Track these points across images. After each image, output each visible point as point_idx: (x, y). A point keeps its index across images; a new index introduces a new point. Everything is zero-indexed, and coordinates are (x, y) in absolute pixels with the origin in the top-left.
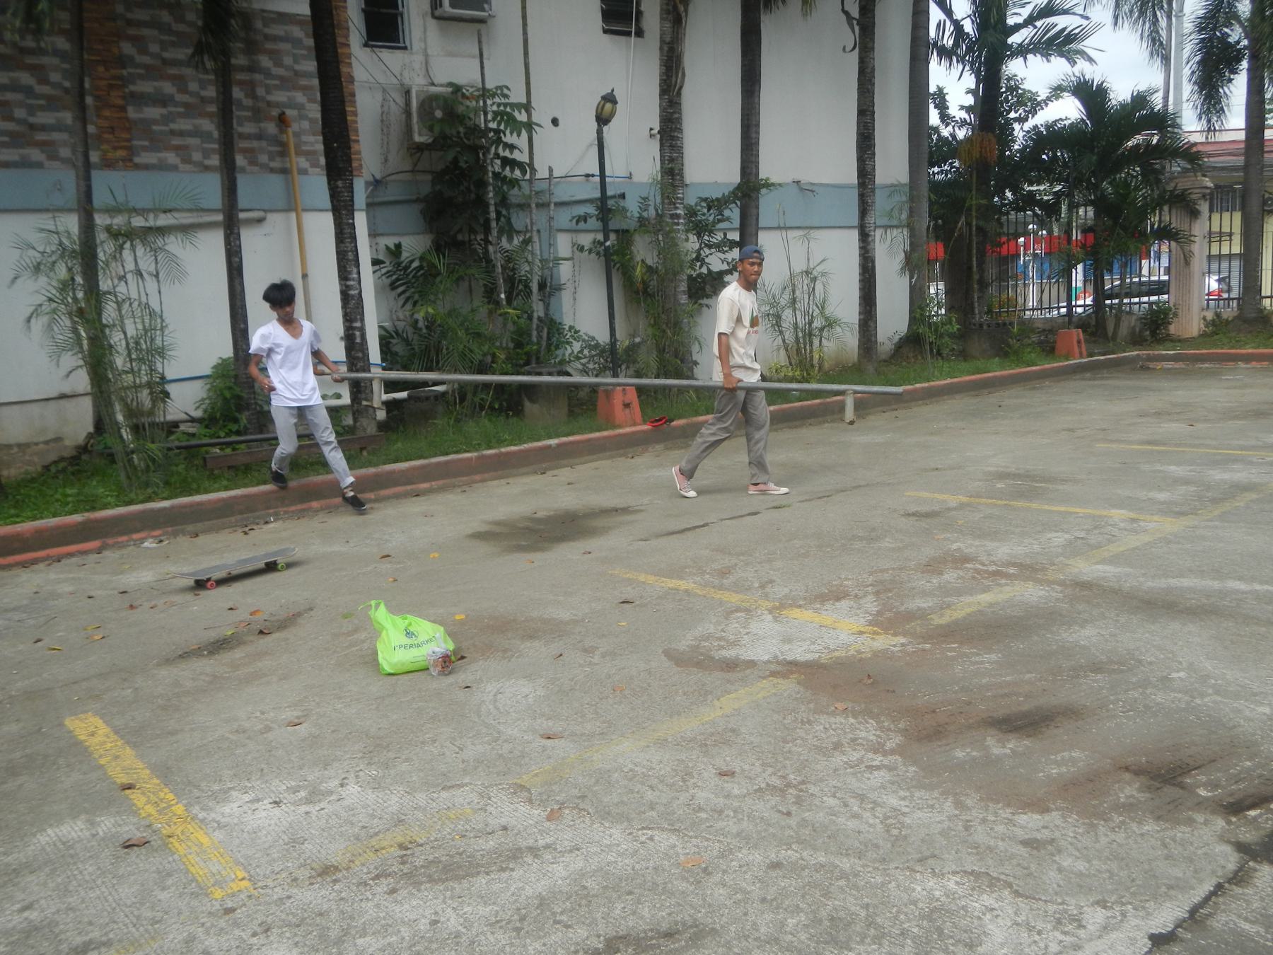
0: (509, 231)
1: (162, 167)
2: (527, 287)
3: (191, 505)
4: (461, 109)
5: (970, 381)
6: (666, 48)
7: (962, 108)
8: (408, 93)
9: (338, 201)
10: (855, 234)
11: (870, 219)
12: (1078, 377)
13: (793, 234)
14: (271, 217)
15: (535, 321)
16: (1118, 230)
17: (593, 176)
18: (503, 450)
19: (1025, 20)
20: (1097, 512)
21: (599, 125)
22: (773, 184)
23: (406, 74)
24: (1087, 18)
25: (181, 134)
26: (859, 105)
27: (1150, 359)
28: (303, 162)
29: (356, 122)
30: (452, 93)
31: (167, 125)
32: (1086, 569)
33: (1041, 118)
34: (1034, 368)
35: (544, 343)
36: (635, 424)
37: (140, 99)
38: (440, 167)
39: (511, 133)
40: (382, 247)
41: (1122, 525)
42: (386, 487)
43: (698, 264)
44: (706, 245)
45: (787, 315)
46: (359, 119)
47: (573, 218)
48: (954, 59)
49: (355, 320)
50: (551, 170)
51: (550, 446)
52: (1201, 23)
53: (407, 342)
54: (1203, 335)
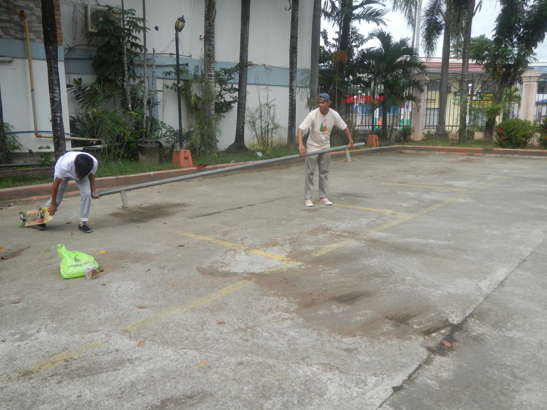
0: (134, 77)
2: (142, 102)
7: (334, 39)
8: (86, 8)
9: (50, 56)
10: (288, 89)
11: (294, 84)
12: (375, 154)
15: (145, 118)
16: (393, 95)
17: (174, 54)
18: (128, 176)
19: (360, 4)
20: (380, 211)
21: (176, 31)
22: (253, 65)
24: (384, 6)
27: (403, 148)
28: (32, 36)
29: (60, 19)
30: (108, 10)
32: (375, 234)
33: (365, 46)
34: (358, 150)
35: (149, 129)
36: (189, 167)
38: (101, 44)
40: (72, 79)
41: (389, 216)
43: (220, 97)
44: (224, 89)
45: (258, 122)
46: (61, 18)
47: (164, 73)
49: (58, 113)
50: (154, 50)
51: (150, 175)
52: (427, 13)
53: (83, 124)
54: (423, 140)
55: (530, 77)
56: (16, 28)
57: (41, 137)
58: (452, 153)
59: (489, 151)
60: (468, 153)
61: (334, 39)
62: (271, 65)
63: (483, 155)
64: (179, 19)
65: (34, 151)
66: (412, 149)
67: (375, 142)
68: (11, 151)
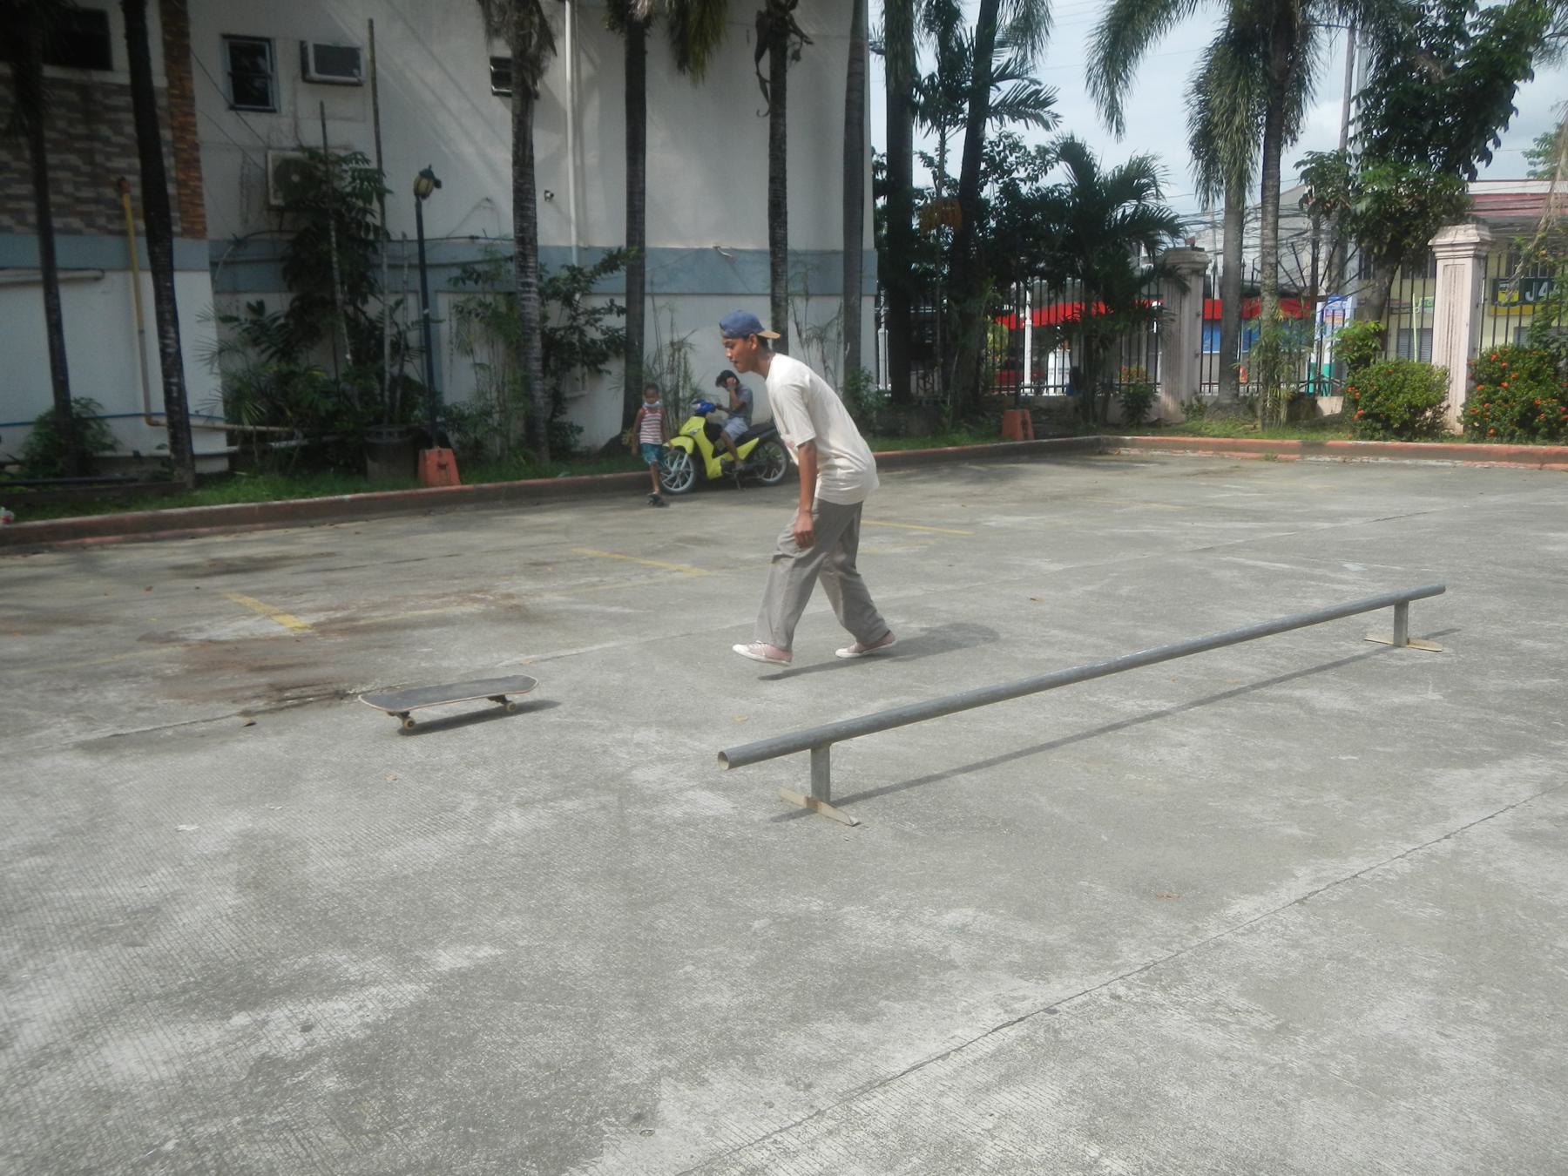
14: (108, 275)
18: (292, 501)
21: (418, 199)
25: (18, 198)
26: (771, 172)
27: (1109, 444)
36: (450, 484)
51: (342, 501)
55: (1452, 245)
56: (110, 212)
58: (1226, 454)
59: (1318, 448)
60: (1263, 455)
62: (735, 247)
63: (1302, 458)
65: (144, 453)
66: (1133, 444)
67: (1019, 427)
68: (95, 454)
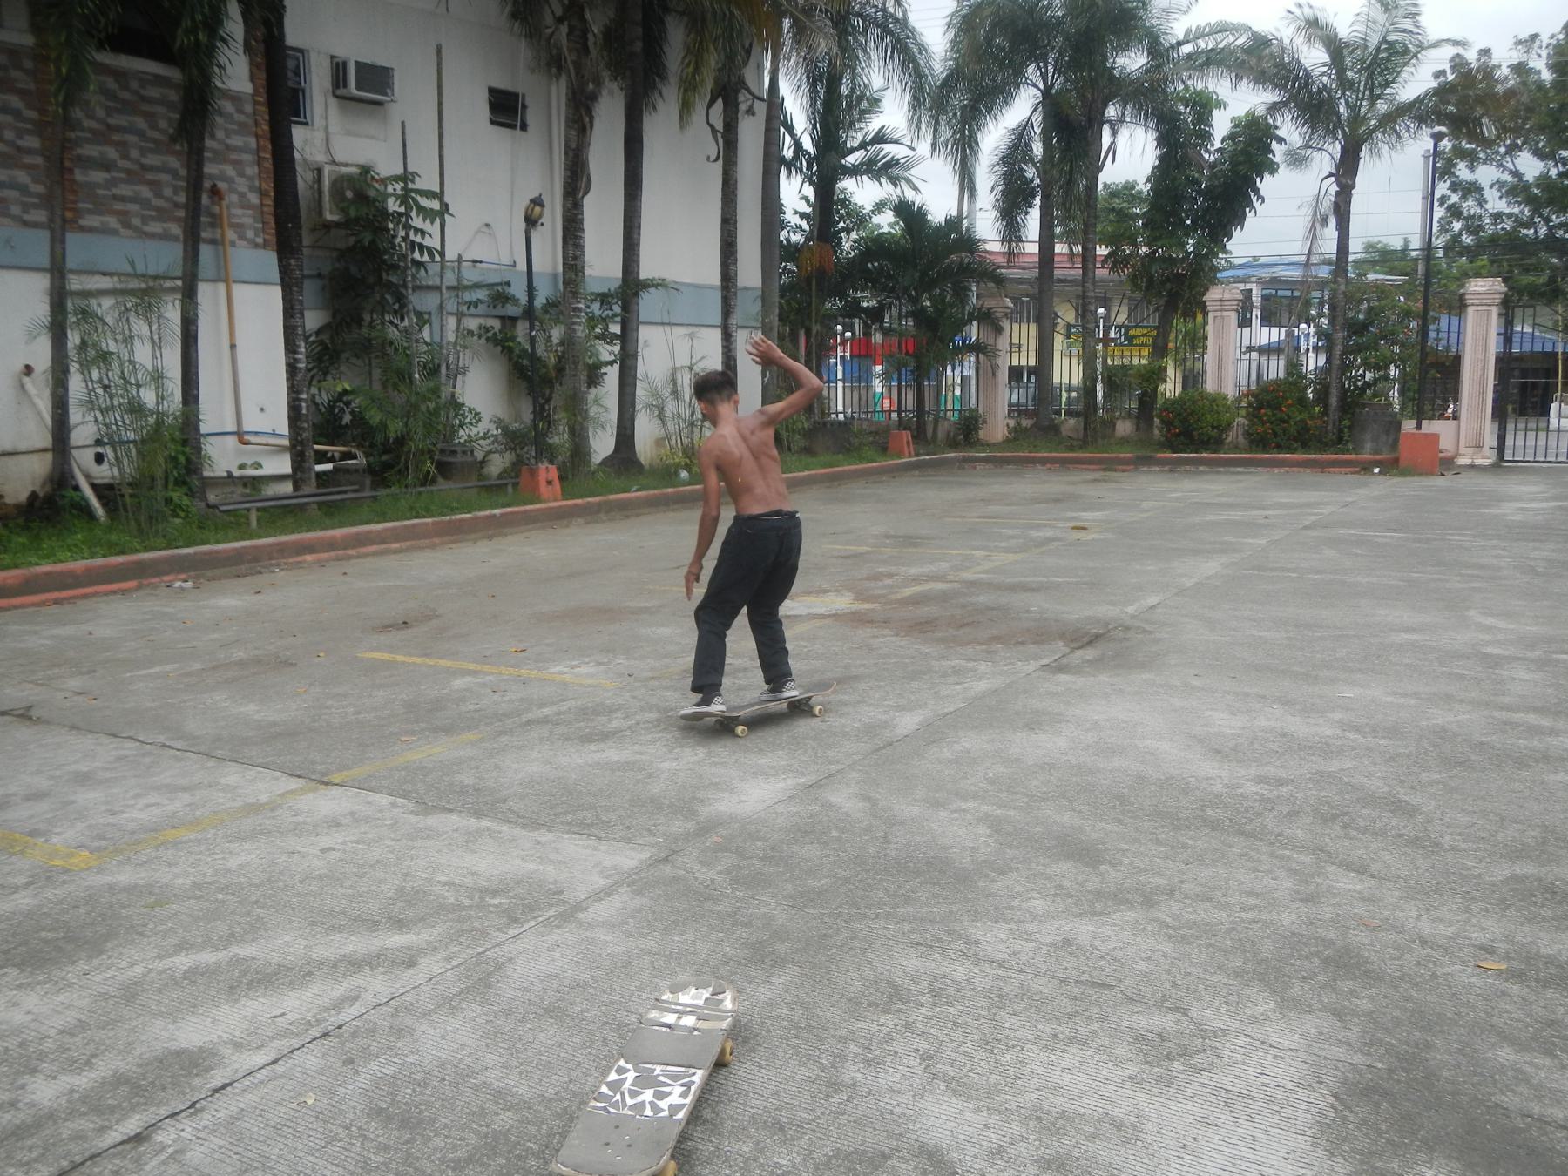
1: (105, 231)
3: (210, 553)
4: (372, 193)
5: (822, 474)
6: (571, 154)
7: (796, 212)
8: (319, 171)
10: (716, 335)
11: (733, 321)
13: (679, 331)
16: (937, 342)
21: (527, 225)
23: (307, 149)
24: (913, 149)
25: (122, 199)
31: (109, 189)
36: (555, 500)
37: (87, 163)
39: (424, 220)
42: (365, 546)
48: (793, 170)
49: (302, 392)
51: (494, 515)
52: (1004, 157)
54: (1007, 441)
57: (247, 443)
58: (1071, 466)
61: (796, 212)
64: (532, 201)
65: (237, 473)
